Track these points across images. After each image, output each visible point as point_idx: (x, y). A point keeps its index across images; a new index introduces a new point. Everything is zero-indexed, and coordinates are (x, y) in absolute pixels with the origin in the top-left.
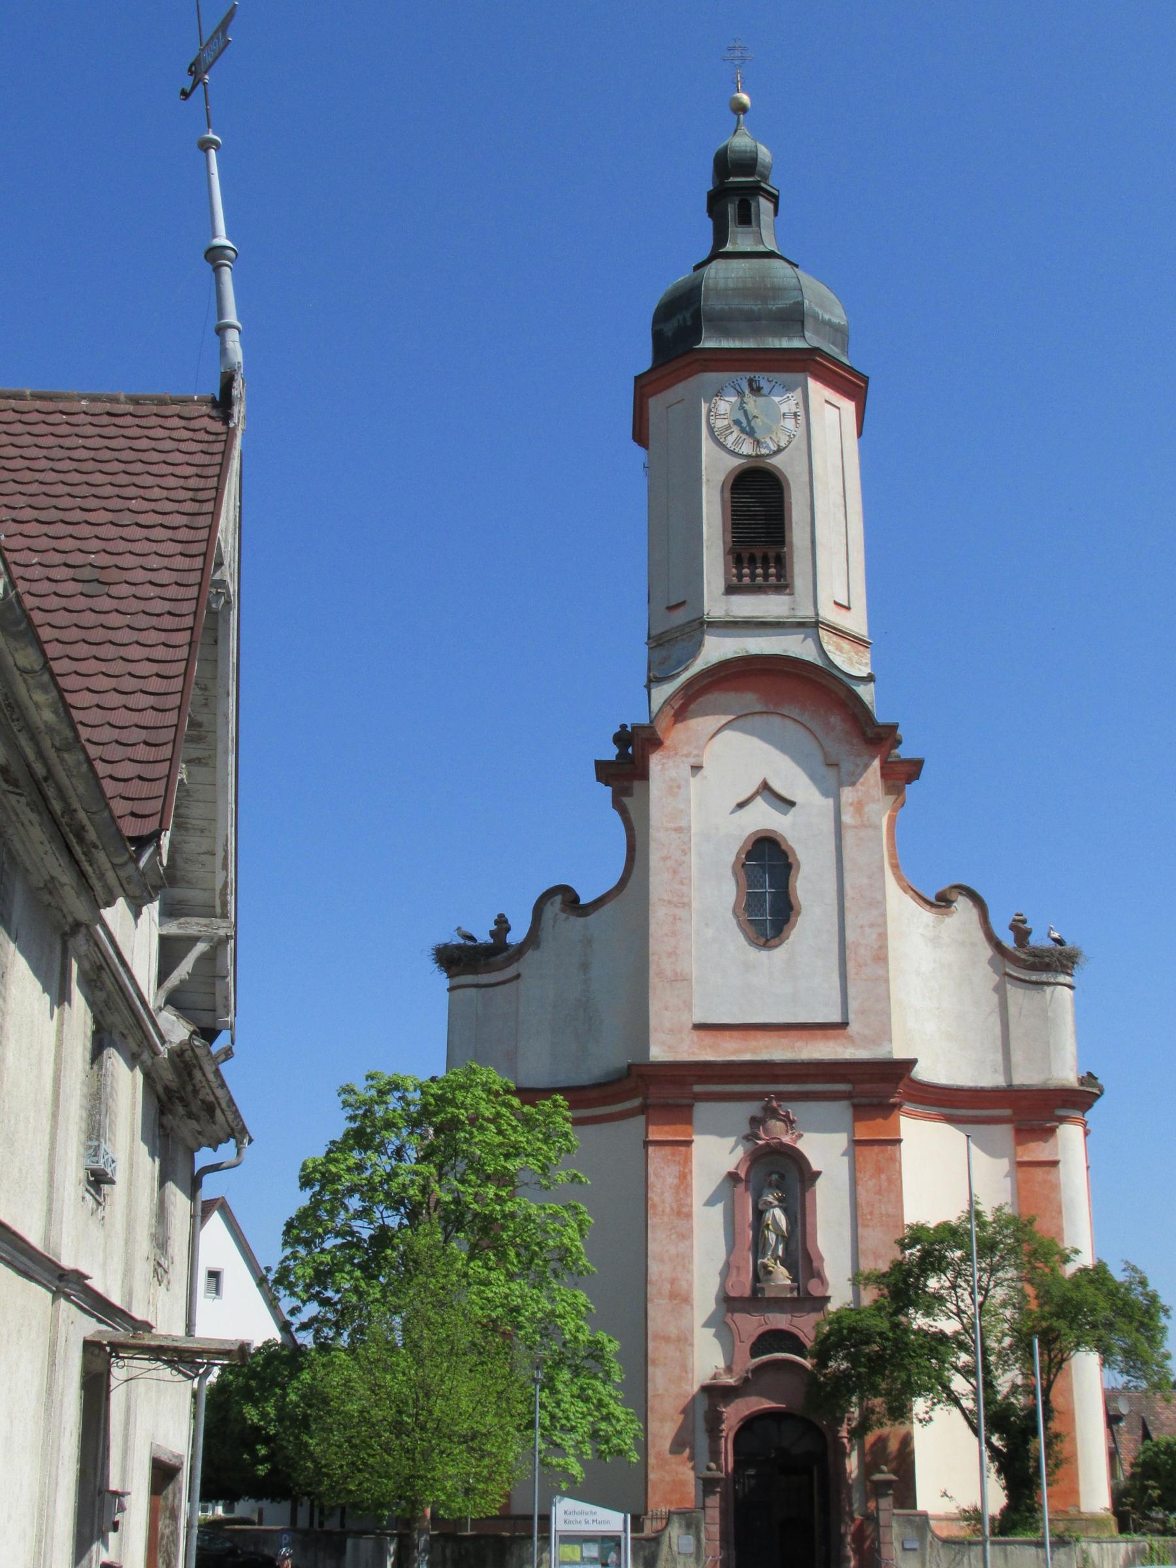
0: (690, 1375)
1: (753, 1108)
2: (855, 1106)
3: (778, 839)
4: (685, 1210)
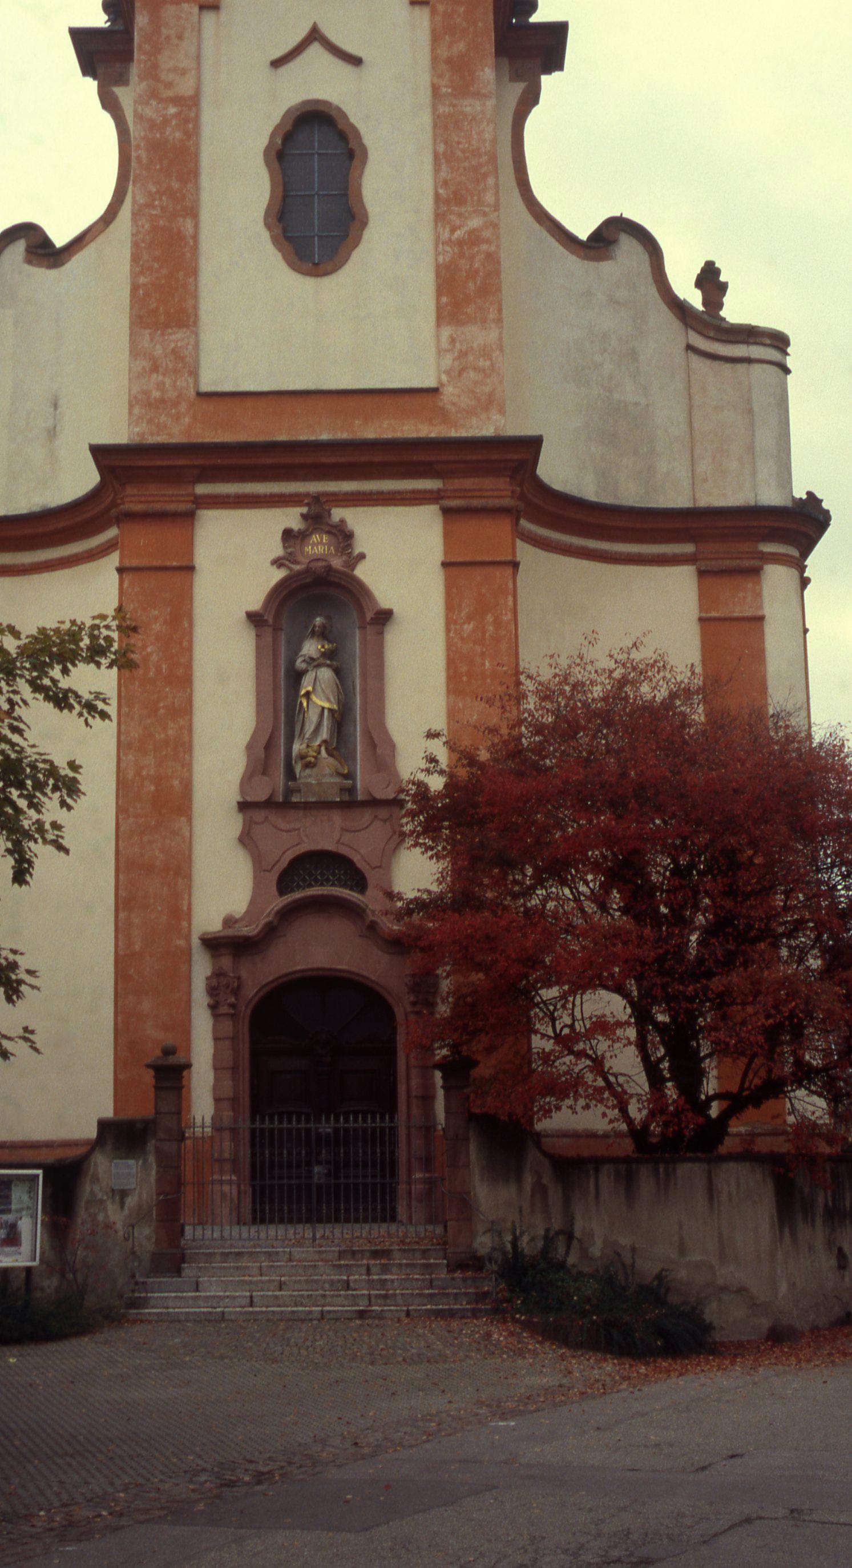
0: (185, 924)
1: (292, 518)
2: (446, 512)
3: (333, 113)
4: (180, 671)
